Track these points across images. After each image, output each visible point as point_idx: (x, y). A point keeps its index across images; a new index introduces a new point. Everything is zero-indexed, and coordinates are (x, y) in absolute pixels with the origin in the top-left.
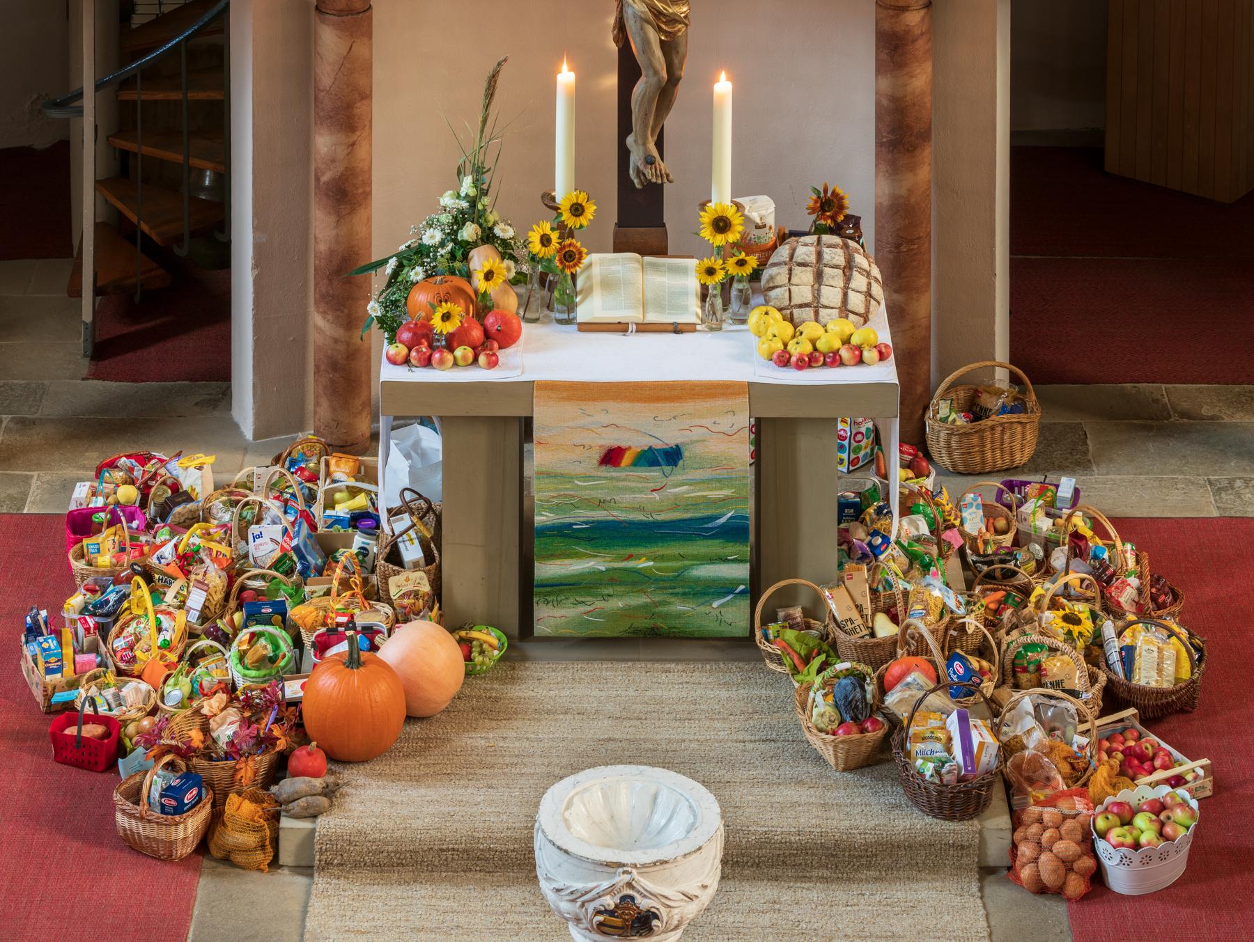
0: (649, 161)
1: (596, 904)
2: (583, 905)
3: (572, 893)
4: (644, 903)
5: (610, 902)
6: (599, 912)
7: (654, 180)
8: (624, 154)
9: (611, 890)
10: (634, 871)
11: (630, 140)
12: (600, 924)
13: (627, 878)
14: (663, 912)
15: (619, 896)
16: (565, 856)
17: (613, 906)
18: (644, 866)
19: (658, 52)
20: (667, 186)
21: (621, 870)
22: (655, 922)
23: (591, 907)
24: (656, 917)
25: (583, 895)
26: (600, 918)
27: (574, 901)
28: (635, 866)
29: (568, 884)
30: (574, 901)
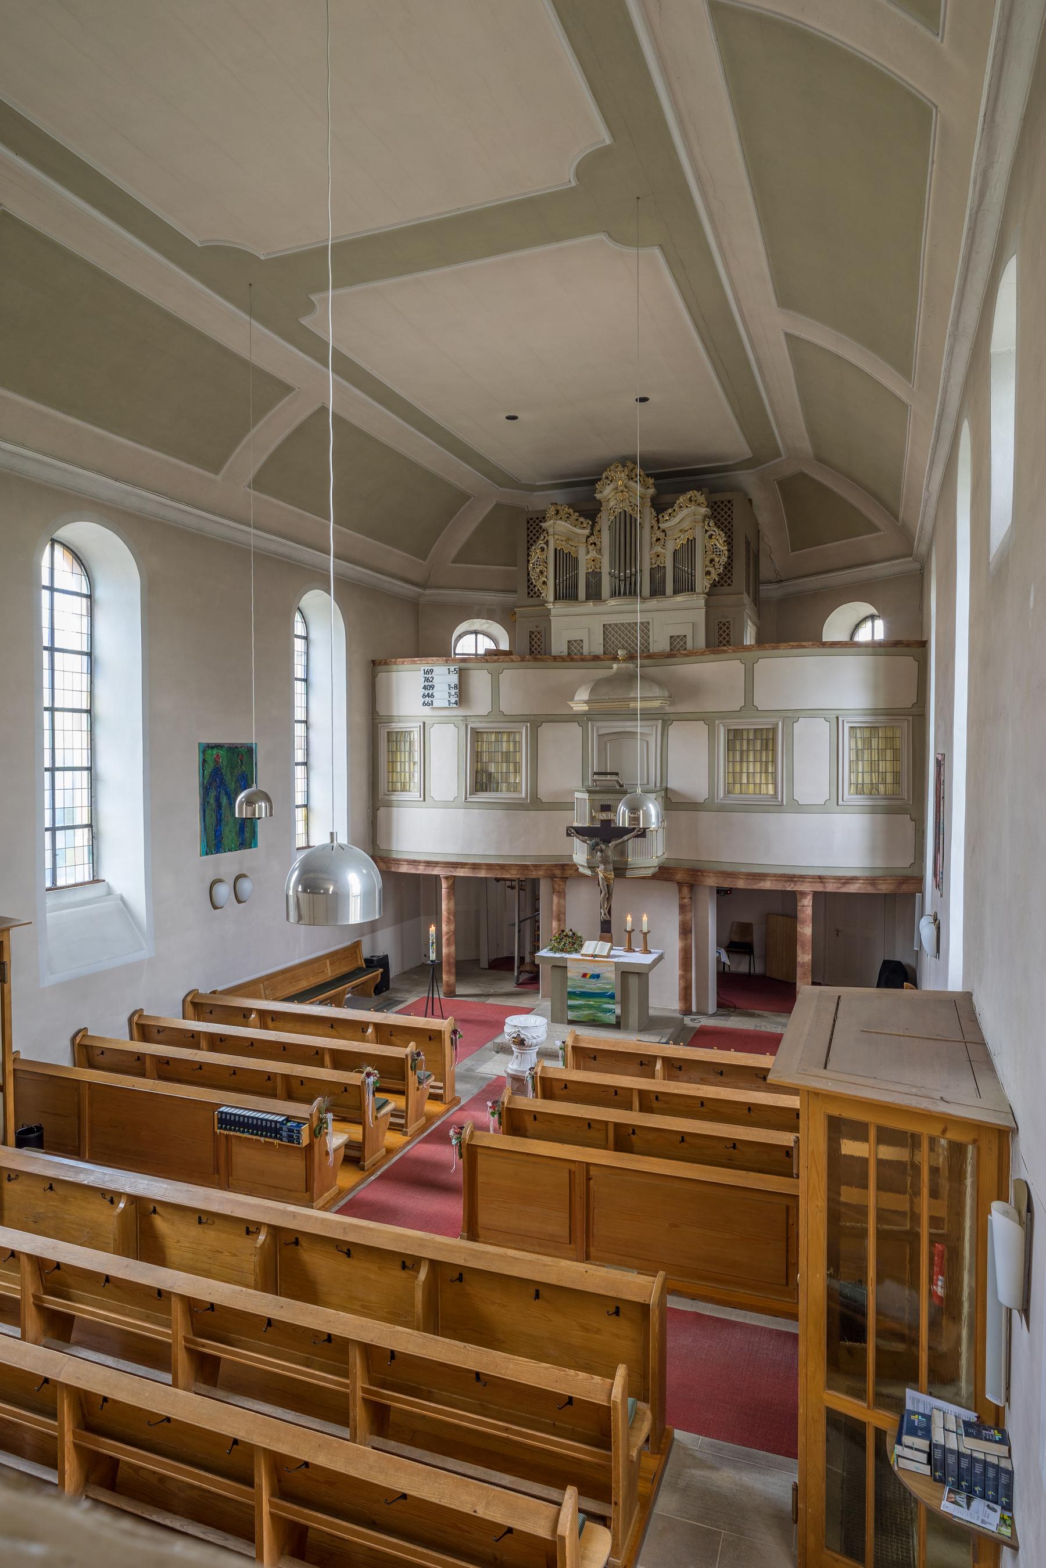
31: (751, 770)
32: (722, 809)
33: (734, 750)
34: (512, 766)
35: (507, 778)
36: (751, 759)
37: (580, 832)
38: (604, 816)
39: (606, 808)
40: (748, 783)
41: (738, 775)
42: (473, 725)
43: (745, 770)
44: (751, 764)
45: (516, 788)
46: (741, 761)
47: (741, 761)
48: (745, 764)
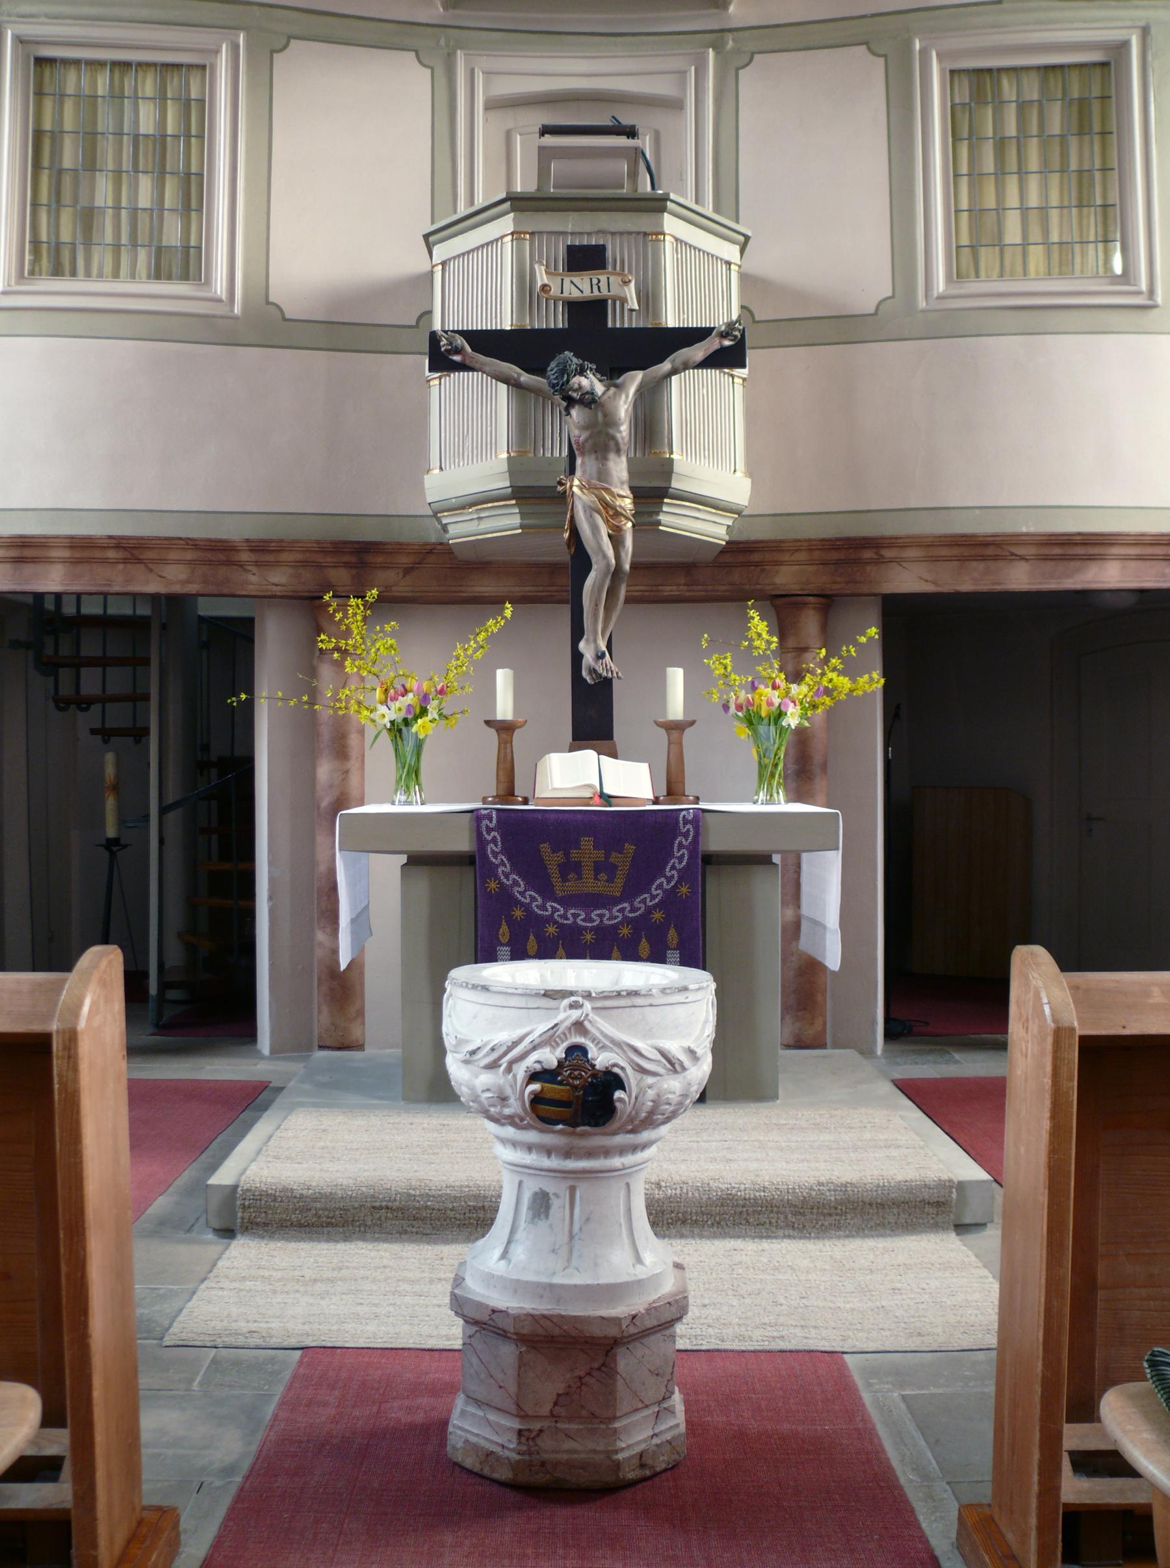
0: (600, 657)
1: (530, 1062)
2: (509, 1069)
3: (493, 1049)
4: (601, 1059)
5: (550, 1057)
6: (533, 1077)
7: (605, 674)
8: (577, 657)
9: (549, 1039)
10: (588, 1005)
11: (582, 645)
12: (536, 1099)
13: (575, 1014)
14: (631, 1077)
15: (565, 1045)
16: (481, 997)
17: (554, 1064)
18: (604, 996)
19: (606, 539)
20: (615, 682)
21: (566, 1002)
22: (618, 1094)
23: (521, 1071)
24: (620, 1084)
25: (510, 1049)
26: (536, 1087)
27: (493, 1066)
28: (588, 996)
29: (485, 1039)
30: (493, 1066)
31: (1034, 200)
32: (946, 325)
33: (975, 139)
34: (171, 189)
35: (157, 228)
36: (1034, 163)
37: (489, 343)
38: (581, 286)
39: (586, 258)
40: (1025, 245)
41: (990, 219)
42: (30, 30)
43: (1012, 200)
44: (1033, 183)
45: (186, 263)
46: (1001, 172)
47: (1001, 172)
48: (1012, 183)
